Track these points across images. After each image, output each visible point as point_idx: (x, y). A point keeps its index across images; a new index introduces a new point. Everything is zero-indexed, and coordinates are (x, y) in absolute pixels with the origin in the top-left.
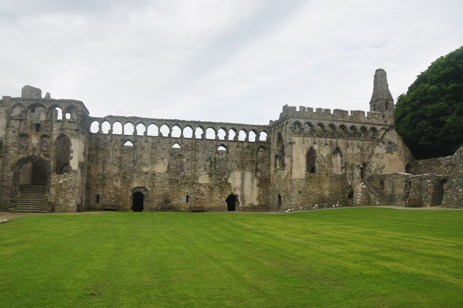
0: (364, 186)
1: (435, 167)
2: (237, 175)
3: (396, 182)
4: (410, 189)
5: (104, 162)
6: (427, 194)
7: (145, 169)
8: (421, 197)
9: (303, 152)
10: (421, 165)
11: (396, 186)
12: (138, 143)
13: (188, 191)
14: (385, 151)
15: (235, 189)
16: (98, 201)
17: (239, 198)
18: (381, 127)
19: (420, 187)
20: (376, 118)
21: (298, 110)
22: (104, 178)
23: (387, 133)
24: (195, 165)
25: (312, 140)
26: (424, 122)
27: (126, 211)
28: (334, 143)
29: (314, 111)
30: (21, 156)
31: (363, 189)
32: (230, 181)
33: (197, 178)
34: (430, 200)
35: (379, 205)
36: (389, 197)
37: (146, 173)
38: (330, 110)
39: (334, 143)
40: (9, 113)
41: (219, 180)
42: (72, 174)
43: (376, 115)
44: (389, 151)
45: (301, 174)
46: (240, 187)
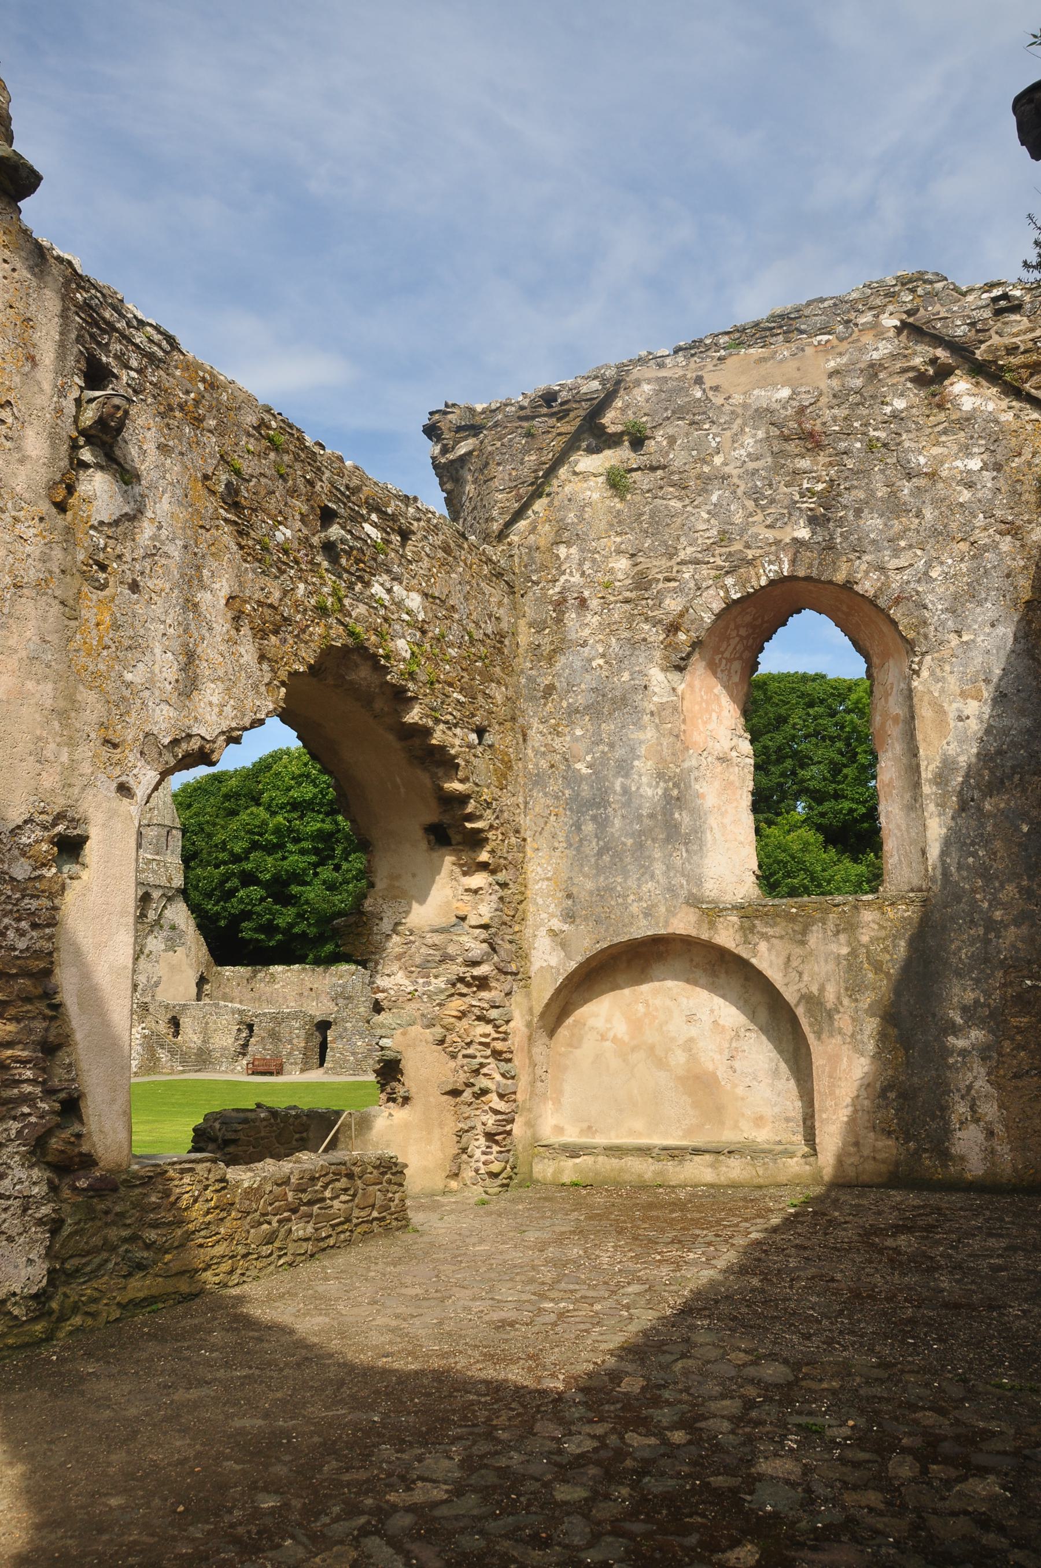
0: (146, 1031)
1: (262, 985)
3: (215, 1023)
4: (251, 1036)
6: (292, 1049)
8: (277, 1056)
10: (228, 980)
11: (215, 1030)
14: (163, 947)
18: (160, 892)
19: (274, 1035)
20: (154, 872)
26: (255, 892)
31: (145, 1037)
34: (299, 1061)
35: (183, 1072)
36: (195, 1054)
43: (154, 863)
44: (171, 946)
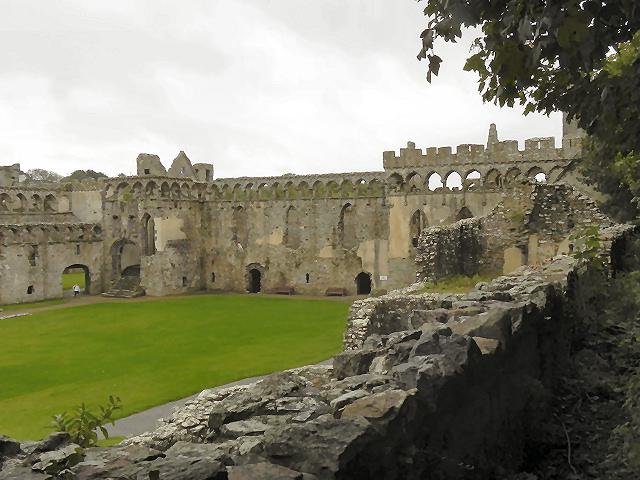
2: (369, 245)
5: (217, 235)
7: (259, 241)
9: (404, 218)
12: (249, 210)
13: (307, 268)
15: (366, 265)
16: (213, 280)
17: (372, 278)
21: (398, 154)
22: (218, 253)
23: (568, 173)
24: (314, 234)
25: (420, 199)
27: (242, 292)
28: (459, 201)
29: (424, 153)
30: (116, 239)
32: (359, 254)
33: (316, 250)
37: (260, 246)
38: (450, 148)
39: (459, 201)
40: (103, 195)
41: (346, 252)
42: (157, 255)
45: (403, 251)
46: (373, 261)
